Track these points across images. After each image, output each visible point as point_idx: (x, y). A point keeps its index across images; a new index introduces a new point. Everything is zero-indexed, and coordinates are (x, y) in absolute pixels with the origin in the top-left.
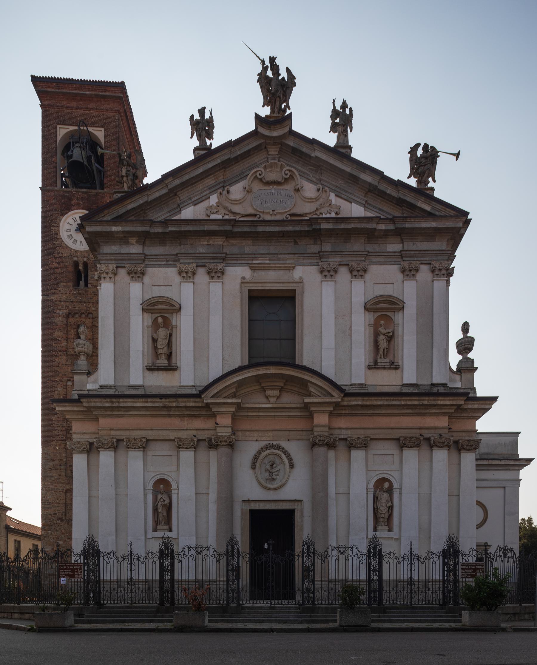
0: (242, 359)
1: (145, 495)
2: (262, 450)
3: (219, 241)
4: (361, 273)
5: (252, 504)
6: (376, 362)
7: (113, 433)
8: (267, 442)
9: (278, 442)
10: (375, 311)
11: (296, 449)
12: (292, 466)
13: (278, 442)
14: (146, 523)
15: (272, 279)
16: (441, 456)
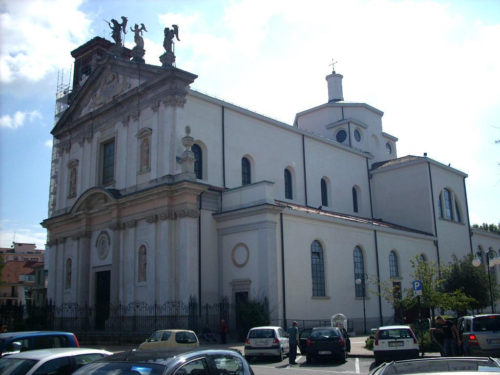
0: (96, 184)
1: (63, 266)
2: (100, 235)
3: (91, 122)
4: (137, 117)
5: (97, 269)
6: (141, 170)
7: (57, 236)
8: (100, 231)
9: (105, 229)
10: (141, 138)
11: (111, 232)
12: (109, 244)
13: (105, 229)
14: (63, 284)
15: (107, 136)
16: (165, 224)
